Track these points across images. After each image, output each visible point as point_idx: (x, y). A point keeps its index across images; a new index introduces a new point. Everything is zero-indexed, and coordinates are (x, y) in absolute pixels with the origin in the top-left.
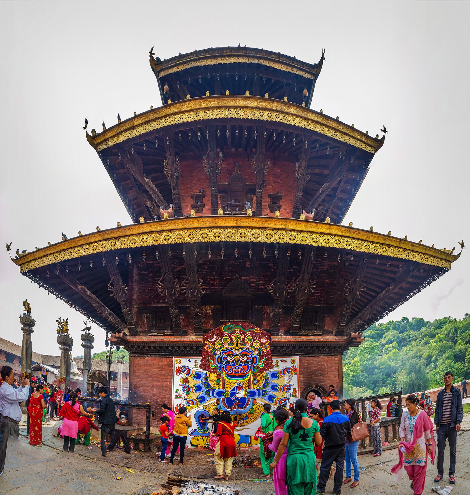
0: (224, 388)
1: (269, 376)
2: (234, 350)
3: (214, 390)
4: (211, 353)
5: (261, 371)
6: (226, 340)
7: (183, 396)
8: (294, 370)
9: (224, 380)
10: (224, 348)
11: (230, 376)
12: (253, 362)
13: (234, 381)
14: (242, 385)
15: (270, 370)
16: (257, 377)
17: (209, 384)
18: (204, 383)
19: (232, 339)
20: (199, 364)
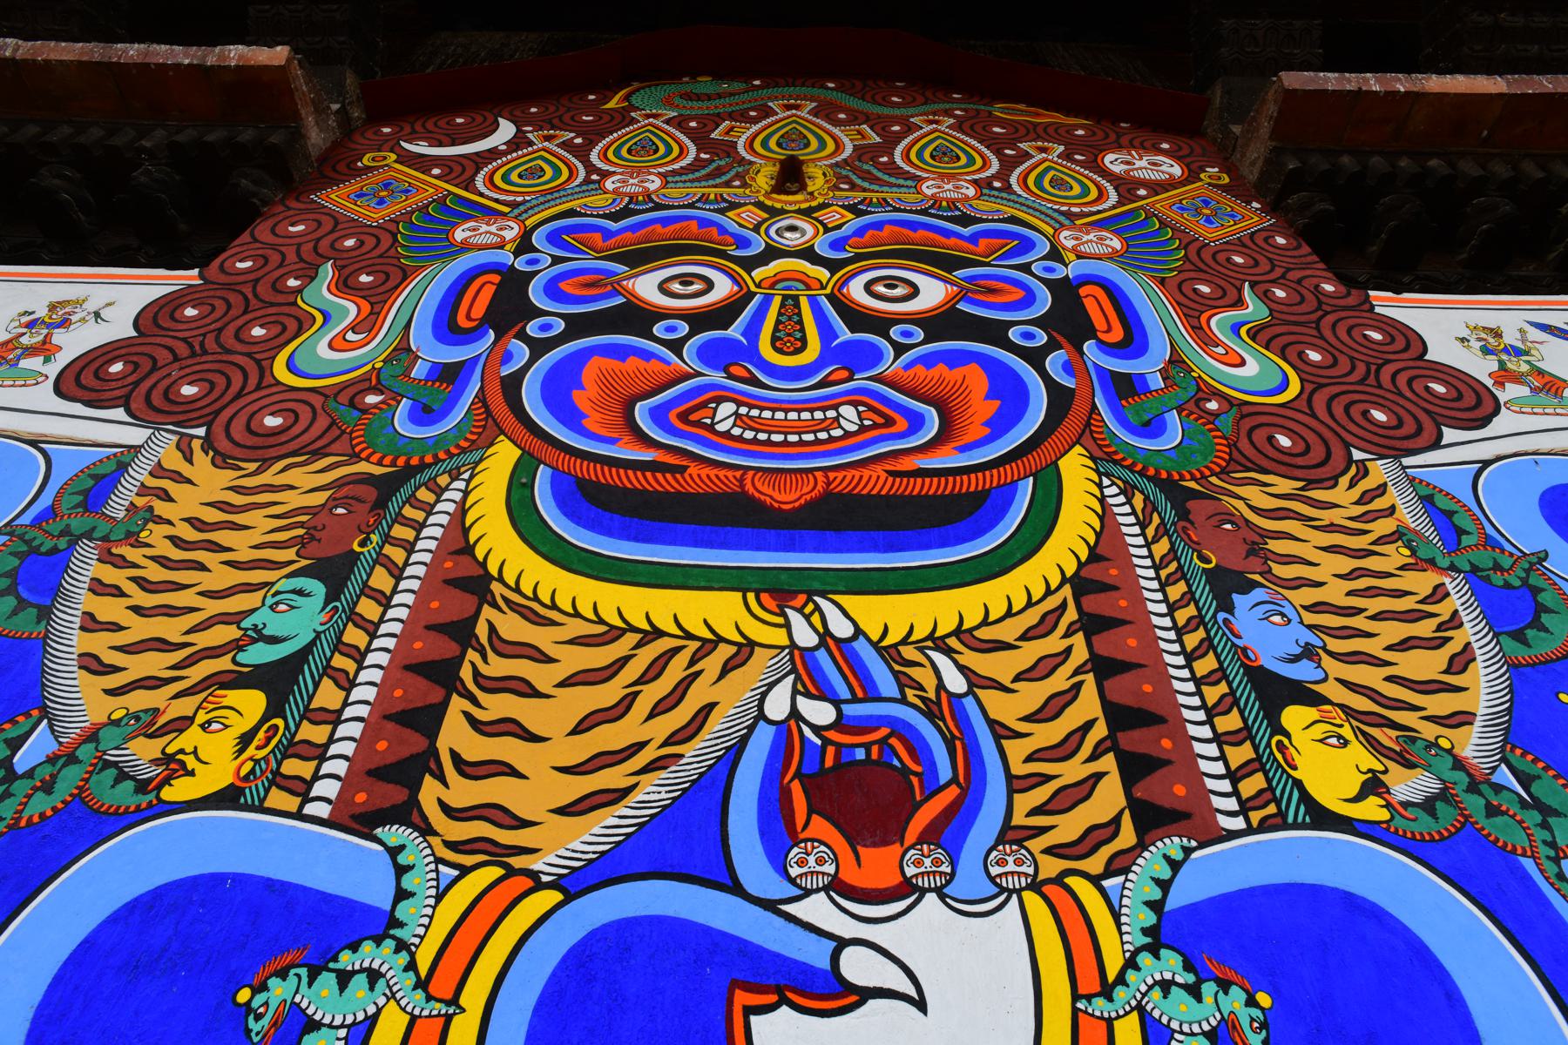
2: (750, 215)
10: (598, 201)
12: (1069, 321)
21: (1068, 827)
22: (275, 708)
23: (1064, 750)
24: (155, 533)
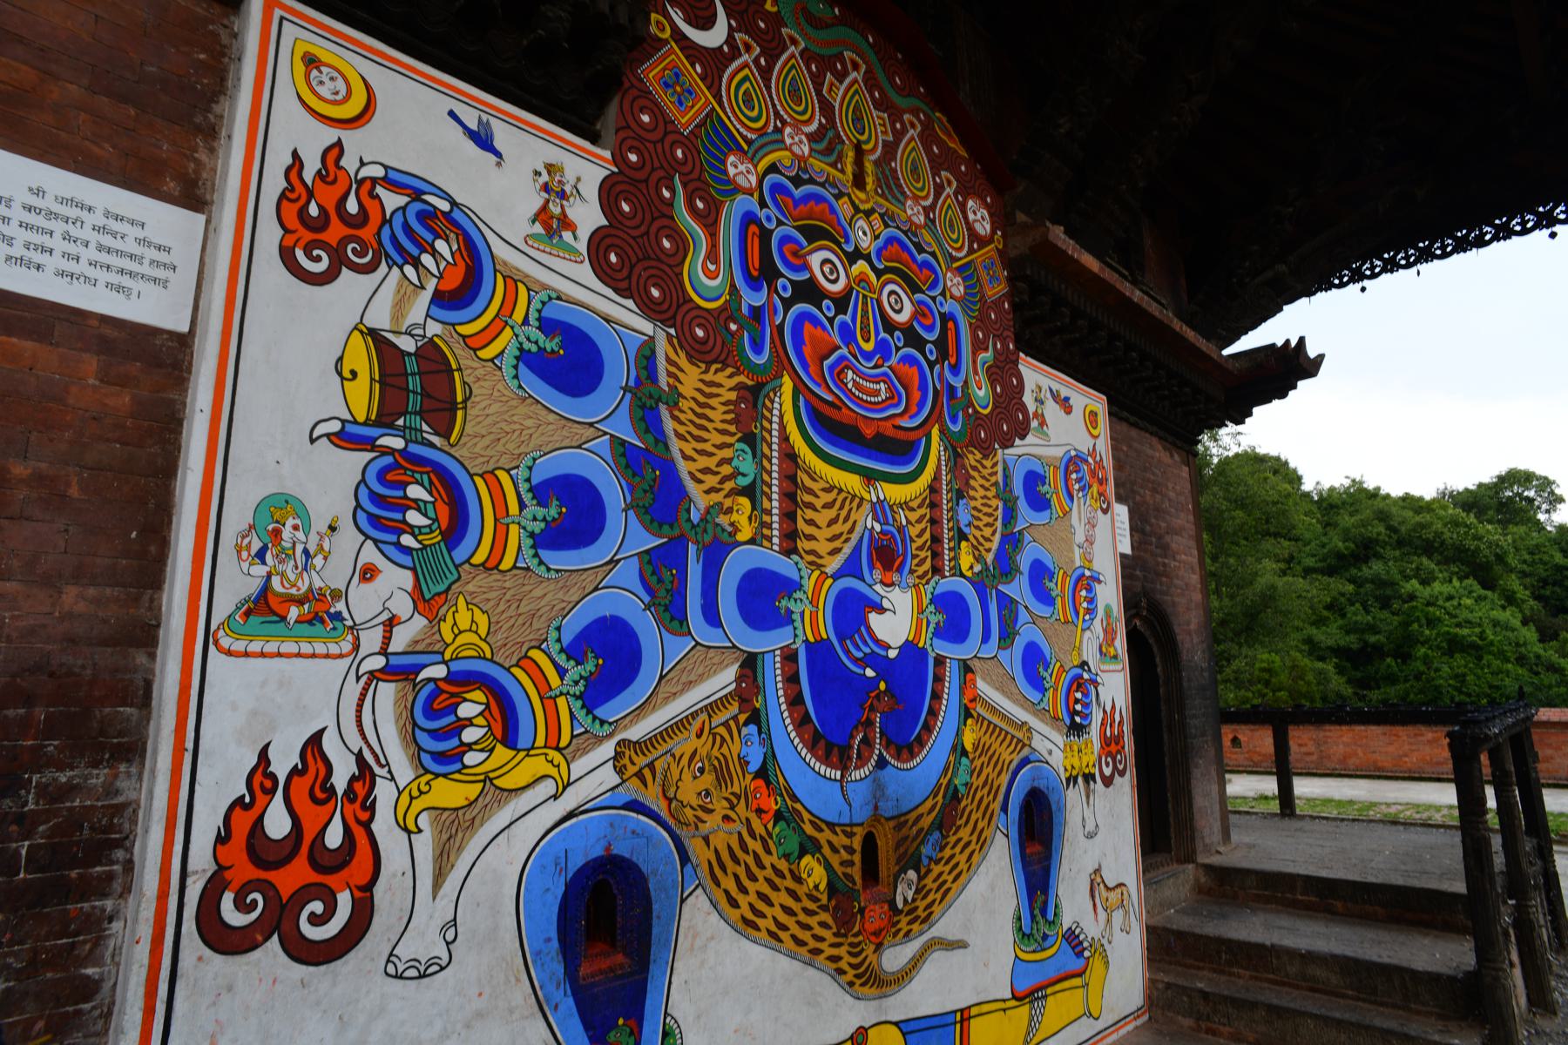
0: (790, 540)
3: (715, 555)
6: (795, 94)
7: (364, 603)
9: (790, 456)
11: (833, 426)
13: (852, 482)
14: (901, 529)
15: (1020, 447)
17: (669, 468)
19: (827, 108)
20: (588, 216)
21: (921, 571)
22: (754, 508)
23: (920, 548)
24: (683, 404)
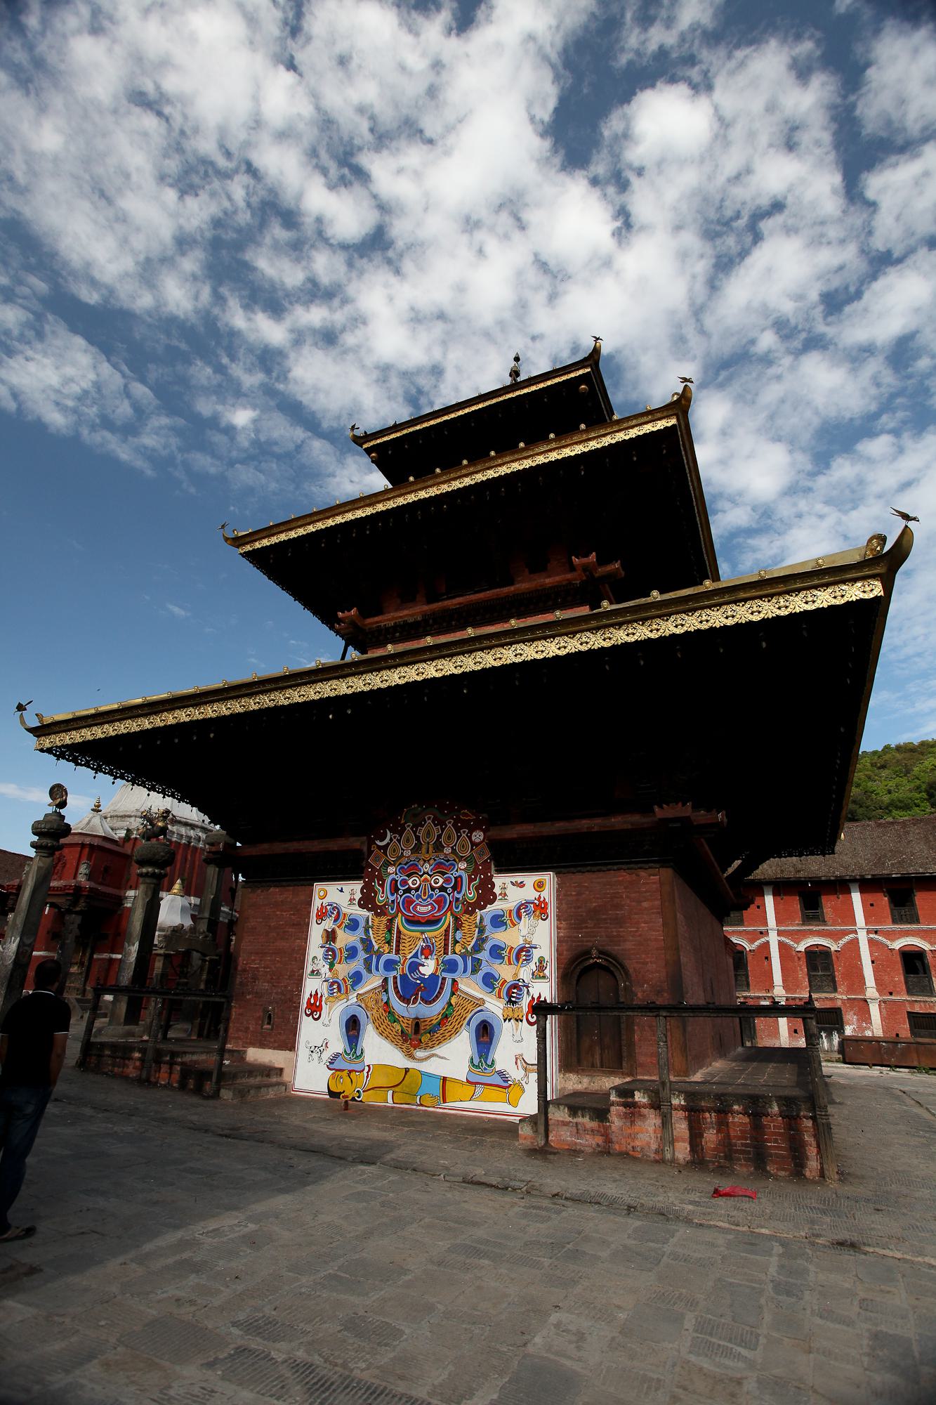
0: (397, 952)
1: (487, 922)
3: (379, 956)
4: (379, 871)
5: (471, 908)
6: (408, 841)
8: (540, 909)
9: (399, 932)
12: (454, 888)
13: (418, 934)
16: (461, 926)
18: (362, 940)
19: (418, 838)
20: (358, 896)
